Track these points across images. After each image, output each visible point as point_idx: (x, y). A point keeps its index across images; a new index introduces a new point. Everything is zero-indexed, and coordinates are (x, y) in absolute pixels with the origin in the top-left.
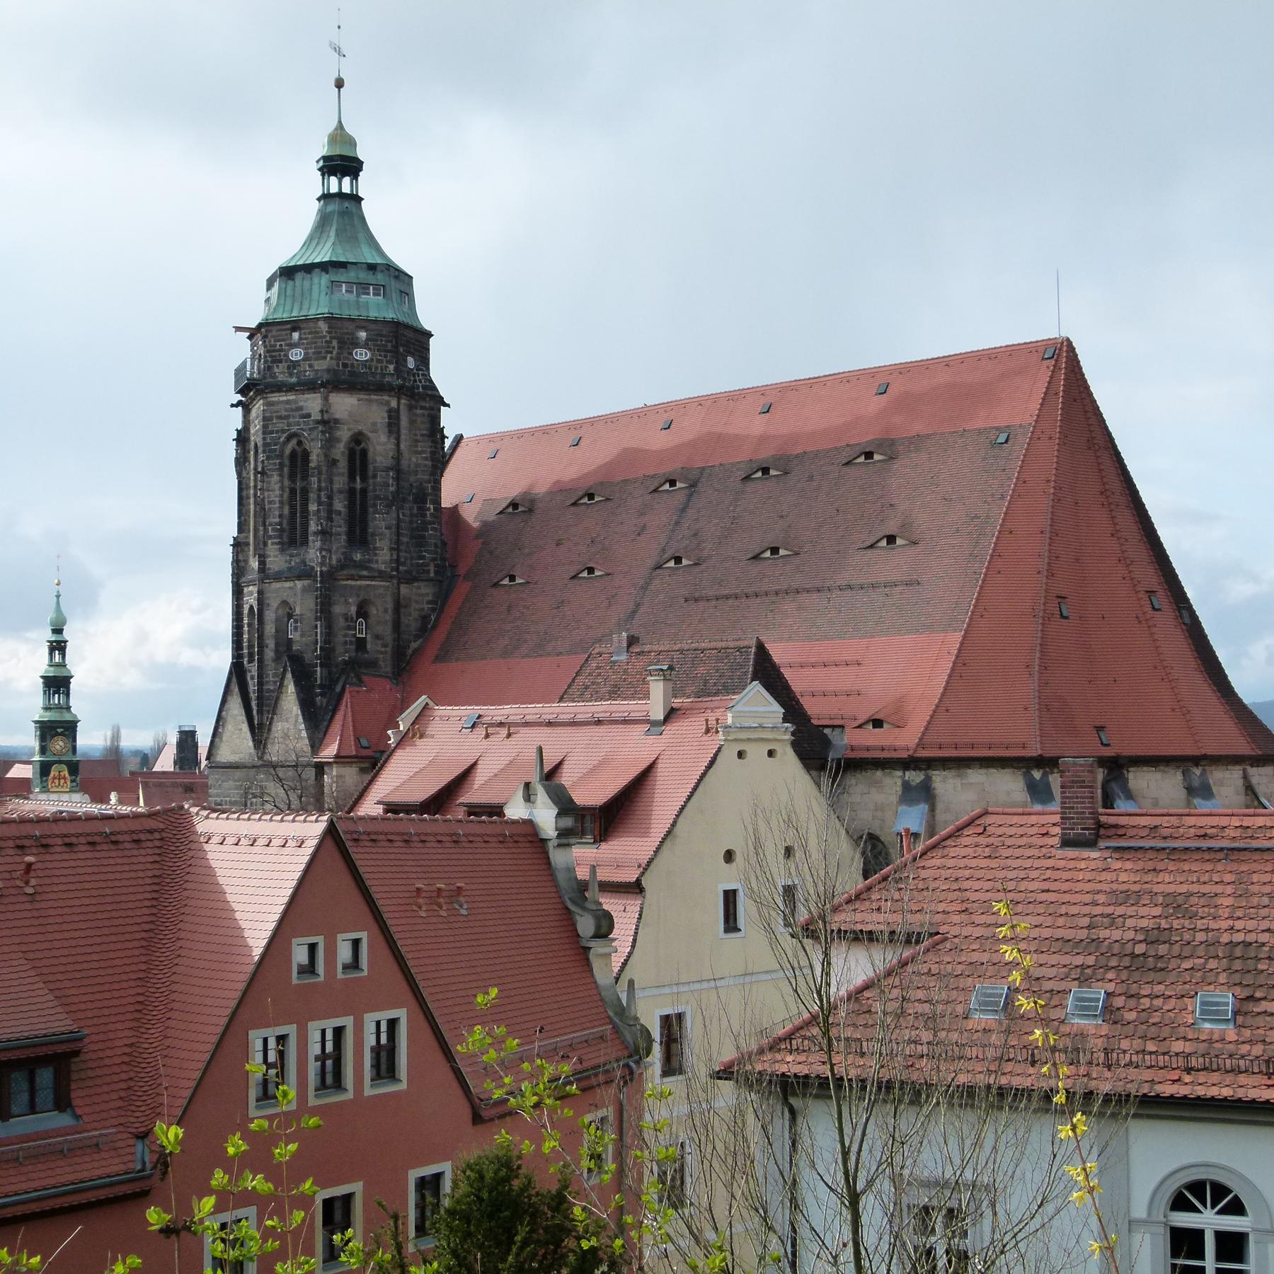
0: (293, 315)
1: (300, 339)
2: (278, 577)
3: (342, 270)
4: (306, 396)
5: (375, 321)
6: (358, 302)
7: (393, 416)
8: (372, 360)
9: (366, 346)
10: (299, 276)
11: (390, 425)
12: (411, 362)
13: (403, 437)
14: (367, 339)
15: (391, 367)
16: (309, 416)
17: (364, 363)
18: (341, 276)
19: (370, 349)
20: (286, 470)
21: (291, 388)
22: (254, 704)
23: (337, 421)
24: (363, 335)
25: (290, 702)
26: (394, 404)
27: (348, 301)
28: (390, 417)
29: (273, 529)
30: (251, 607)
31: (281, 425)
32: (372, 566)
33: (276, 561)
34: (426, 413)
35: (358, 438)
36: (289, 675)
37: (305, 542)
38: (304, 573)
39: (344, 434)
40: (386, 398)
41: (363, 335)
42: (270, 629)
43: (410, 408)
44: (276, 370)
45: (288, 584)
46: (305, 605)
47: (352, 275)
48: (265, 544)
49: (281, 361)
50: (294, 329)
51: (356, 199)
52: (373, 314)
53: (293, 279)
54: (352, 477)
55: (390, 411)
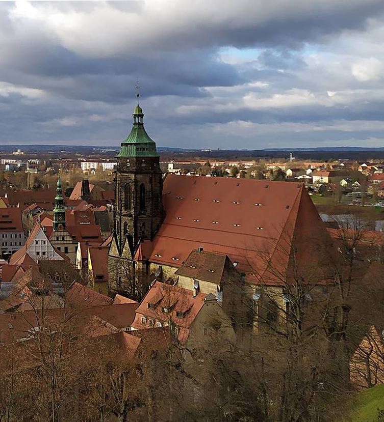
2: (124, 216)
7: (151, 179)
10: (129, 146)
11: (150, 181)
18: (139, 146)
21: (127, 173)
23: (138, 181)
25: (127, 244)
31: (125, 181)
33: (124, 212)
35: (143, 184)
37: (130, 208)
38: (130, 216)
41: (144, 160)
42: (123, 228)
46: (131, 224)
50: (128, 159)
54: (141, 194)
55: (150, 178)
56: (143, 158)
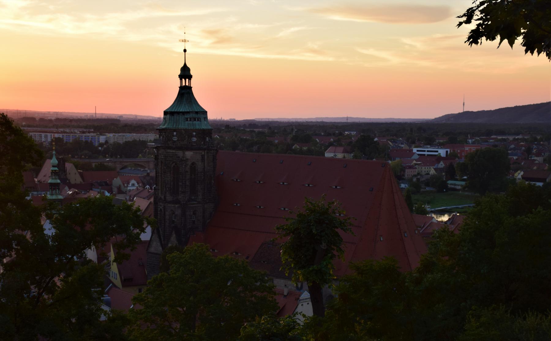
0: (174, 127)
1: (176, 134)
3: (189, 114)
4: (178, 151)
5: (198, 130)
6: (193, 123)
7: (203, 157)
8: (197, 141)
9: (195, 136)
12: (207, 139)
13: (205, 162)
14: (196, 135)
15: (202, 142)
16: (179, 157)
17: (195, 142)
19: (196, 138)
20: (172, 172)
21: (174, 149)
22: (162, 237)
23: (187, 159)
24: (194, 133)
26: (203, 153)
27: (190, 123)
28: (202, 157)
29: (168, 189)
30: (161, 210)
32: (198, 200)
33: (169, 198)
34: (212, 154)
35: (193, 164)
36: (174, 232)
39: (189, 163)
40: (201, 152)
41: (194, 133)
43: (207, 153)
44: (169, 143)
45: (173, 205)
46: (178, 212)
47: (191, 115)
48: (166, 193)
49: (171, 140)
51: (190, 88)
52: (197, 127)
53: (174, 116)
55: (202, 156)
56: (195, 130)
